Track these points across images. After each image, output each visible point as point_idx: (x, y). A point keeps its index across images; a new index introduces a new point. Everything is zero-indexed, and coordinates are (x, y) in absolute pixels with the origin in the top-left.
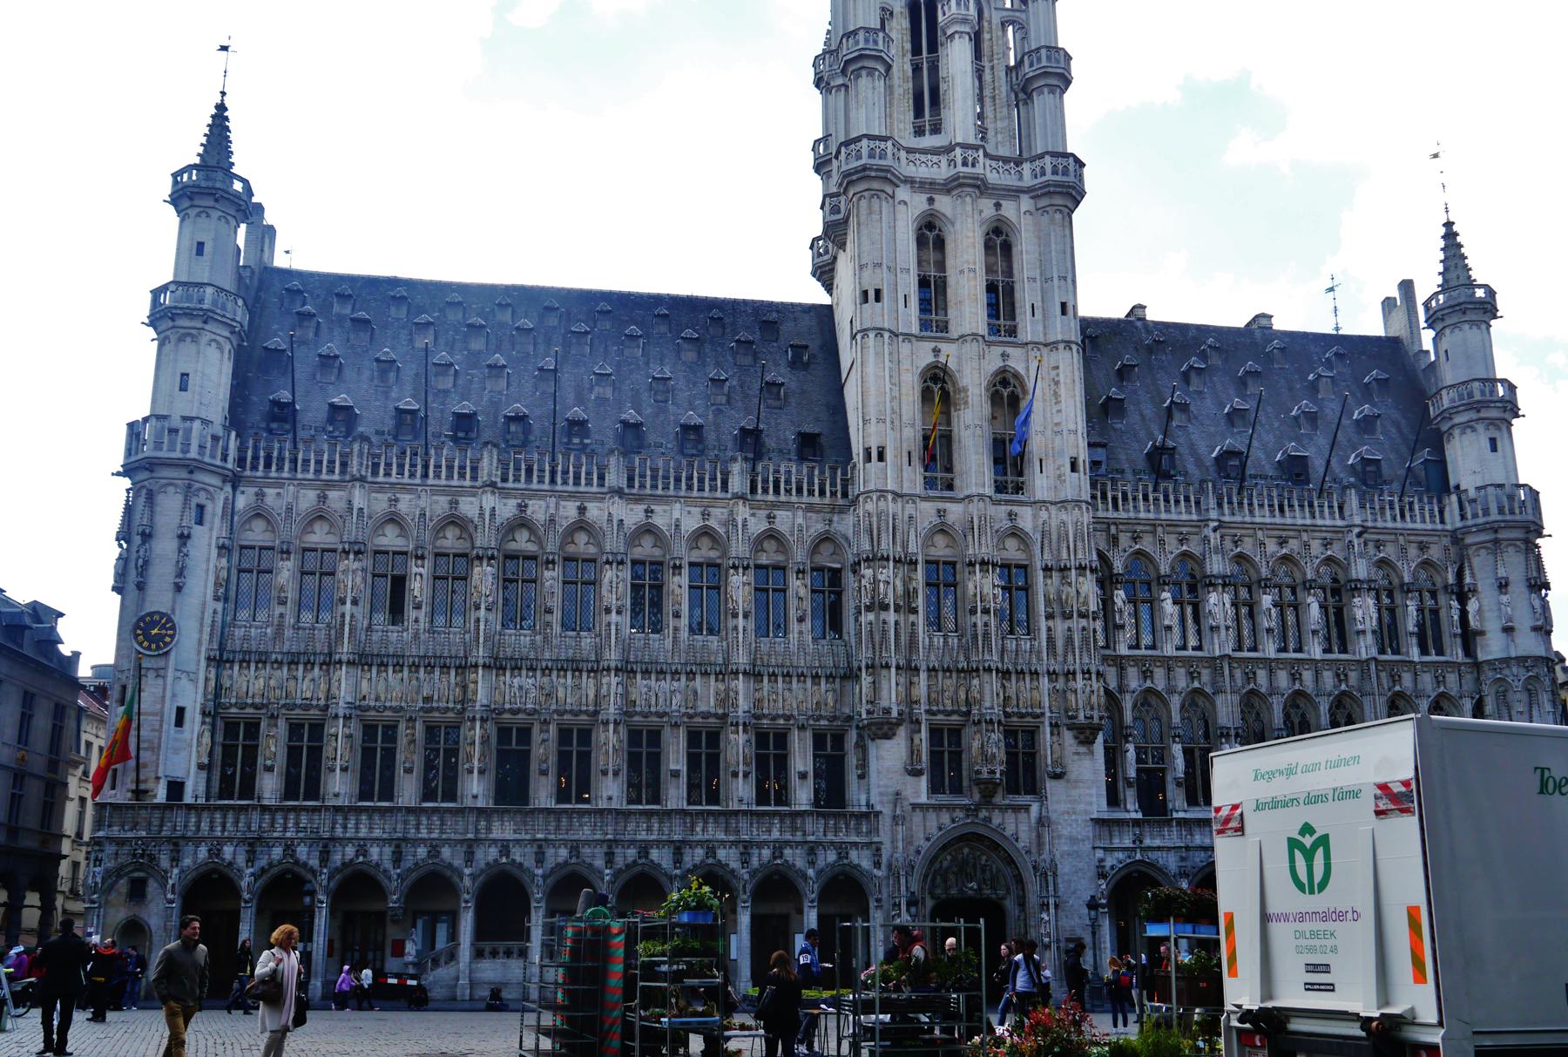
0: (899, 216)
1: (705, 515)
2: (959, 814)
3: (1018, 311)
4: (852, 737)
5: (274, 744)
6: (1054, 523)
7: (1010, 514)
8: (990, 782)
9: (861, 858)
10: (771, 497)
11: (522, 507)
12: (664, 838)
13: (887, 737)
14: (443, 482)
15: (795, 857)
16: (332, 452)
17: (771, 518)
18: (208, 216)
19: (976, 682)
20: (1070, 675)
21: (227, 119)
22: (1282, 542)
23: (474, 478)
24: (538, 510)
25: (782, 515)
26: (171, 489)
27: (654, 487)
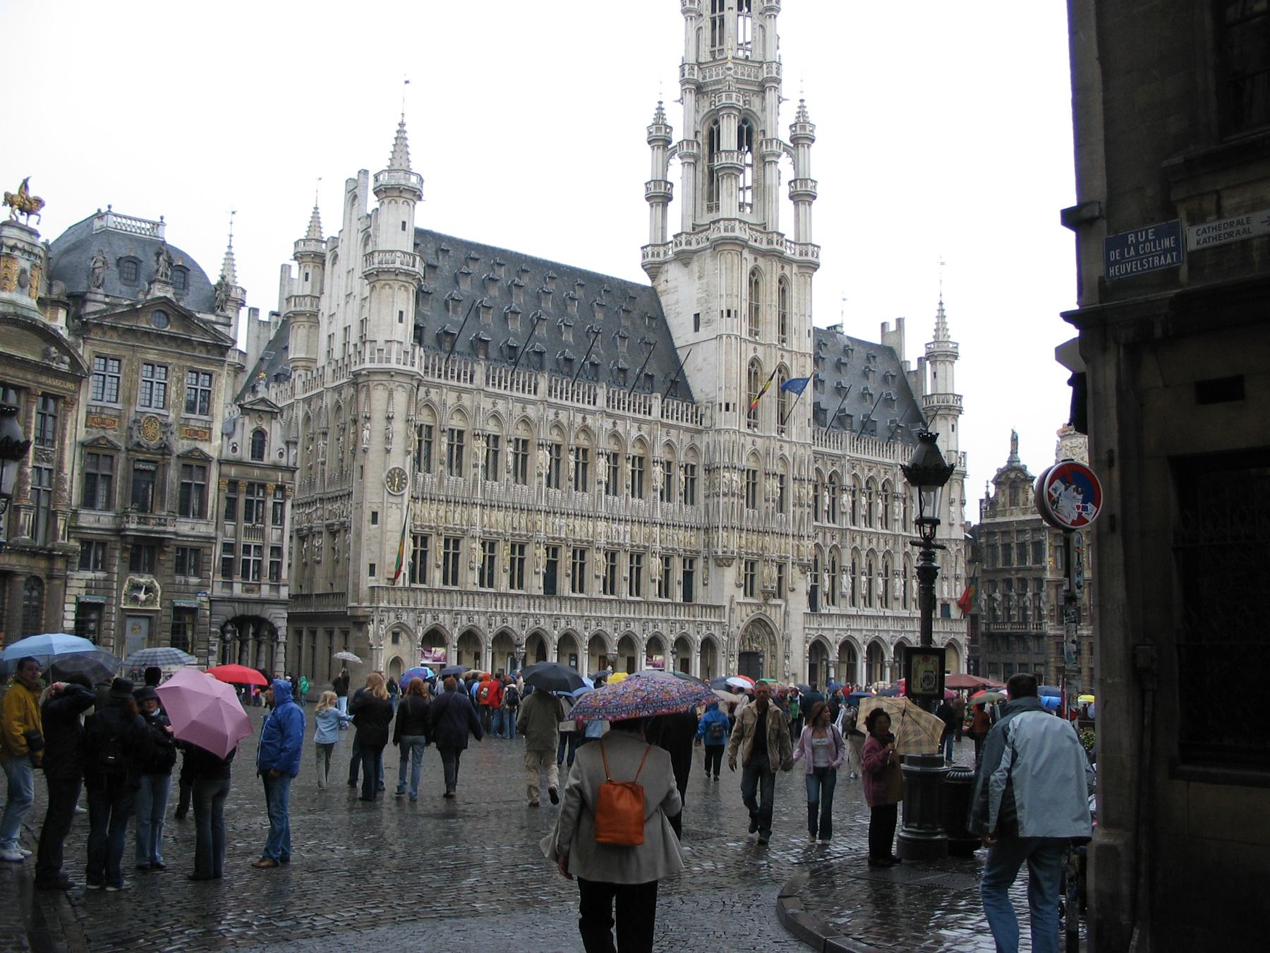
0: (744, 267)
1: (639, 429)
2: (754, 608)
3: (787, 330)
4: (699, 564)
5: (436, 549)
6: (799, 453)
7: (781, 447)
8: (769, 592)
9: (716, 632)
10: (670, 421)
11: (557, 414)
12: (637, 616)
13: (729, 566)
14: (521, 395)
15: (690, 630)
16: (466, 367)
17: (668, 433)
18: (408, 204)
19: (767, 538)
20: (801, 537)
21: (405, 132)
22: (869, 470)
23: (535, 393)
24: (563, 416)
25: (673, 432)
26: (400, 388)
27: (619, 408)
